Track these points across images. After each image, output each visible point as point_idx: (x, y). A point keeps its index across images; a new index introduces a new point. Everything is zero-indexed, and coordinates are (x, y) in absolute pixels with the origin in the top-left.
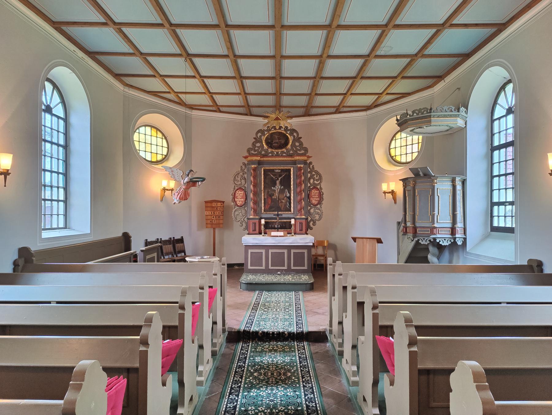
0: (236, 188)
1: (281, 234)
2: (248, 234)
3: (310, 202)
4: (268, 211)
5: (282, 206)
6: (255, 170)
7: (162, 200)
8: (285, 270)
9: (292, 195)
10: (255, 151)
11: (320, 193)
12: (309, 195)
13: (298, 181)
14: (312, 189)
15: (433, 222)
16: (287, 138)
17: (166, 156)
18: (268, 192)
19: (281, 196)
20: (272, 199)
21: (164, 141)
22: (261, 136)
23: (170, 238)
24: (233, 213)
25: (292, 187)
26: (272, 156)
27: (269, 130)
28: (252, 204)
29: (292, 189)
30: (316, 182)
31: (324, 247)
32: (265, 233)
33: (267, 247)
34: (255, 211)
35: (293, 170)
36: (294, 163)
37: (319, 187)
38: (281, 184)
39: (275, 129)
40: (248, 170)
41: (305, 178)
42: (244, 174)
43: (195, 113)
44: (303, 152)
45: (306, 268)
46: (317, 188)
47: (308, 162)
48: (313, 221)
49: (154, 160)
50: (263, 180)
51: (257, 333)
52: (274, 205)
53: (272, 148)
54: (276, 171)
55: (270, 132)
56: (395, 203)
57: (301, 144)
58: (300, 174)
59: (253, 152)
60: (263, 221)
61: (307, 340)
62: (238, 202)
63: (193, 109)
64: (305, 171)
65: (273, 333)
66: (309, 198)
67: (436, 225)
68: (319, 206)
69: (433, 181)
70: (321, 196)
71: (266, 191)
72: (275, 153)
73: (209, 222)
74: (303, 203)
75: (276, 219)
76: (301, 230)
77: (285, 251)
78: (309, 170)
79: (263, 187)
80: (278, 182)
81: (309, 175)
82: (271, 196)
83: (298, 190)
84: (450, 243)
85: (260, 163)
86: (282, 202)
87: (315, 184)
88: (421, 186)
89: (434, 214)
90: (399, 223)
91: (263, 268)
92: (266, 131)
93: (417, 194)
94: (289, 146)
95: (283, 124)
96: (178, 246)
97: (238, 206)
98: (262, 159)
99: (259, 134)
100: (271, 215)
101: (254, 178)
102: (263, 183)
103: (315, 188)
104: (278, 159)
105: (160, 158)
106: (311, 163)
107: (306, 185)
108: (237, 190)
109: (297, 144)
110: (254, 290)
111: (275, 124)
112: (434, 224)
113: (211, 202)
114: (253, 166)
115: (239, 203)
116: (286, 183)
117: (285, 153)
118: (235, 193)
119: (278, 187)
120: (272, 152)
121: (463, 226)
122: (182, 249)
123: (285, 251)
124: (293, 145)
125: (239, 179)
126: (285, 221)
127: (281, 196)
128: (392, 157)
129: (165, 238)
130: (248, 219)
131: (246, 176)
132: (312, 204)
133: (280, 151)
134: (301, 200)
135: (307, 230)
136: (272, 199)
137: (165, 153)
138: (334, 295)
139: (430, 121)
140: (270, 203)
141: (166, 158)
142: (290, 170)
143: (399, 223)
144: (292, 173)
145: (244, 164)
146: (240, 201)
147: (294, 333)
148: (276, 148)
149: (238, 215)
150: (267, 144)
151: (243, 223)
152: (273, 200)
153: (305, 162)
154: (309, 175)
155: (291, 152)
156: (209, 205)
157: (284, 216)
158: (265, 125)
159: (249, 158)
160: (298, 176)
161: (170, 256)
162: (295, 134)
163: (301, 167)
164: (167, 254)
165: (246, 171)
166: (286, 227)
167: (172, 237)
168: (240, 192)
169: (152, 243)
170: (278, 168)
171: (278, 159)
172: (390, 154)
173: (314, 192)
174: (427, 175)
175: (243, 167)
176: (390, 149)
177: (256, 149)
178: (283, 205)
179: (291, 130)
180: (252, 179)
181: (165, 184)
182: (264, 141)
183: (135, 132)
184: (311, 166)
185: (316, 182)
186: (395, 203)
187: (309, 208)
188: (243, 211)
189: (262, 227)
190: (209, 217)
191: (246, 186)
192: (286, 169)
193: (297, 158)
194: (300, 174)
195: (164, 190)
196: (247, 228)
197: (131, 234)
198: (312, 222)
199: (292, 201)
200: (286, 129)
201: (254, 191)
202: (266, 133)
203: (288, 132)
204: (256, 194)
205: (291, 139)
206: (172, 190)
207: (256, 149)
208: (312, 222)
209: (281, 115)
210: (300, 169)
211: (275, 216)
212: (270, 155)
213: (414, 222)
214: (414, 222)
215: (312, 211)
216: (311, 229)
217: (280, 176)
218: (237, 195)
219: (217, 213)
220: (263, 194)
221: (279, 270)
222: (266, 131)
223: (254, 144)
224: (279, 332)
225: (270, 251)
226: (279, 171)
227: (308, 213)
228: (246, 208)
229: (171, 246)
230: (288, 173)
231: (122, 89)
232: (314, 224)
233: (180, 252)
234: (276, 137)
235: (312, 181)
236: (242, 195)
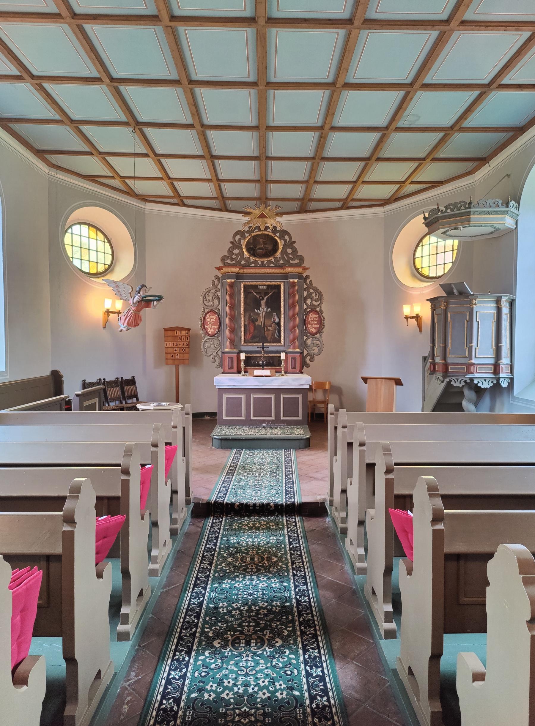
0: (207, 311)
1: (268, 372)
2: (223, 373)
3: (306, 330)
4: (248, 342)
6: (231, 285)
7: (105, 327)
8: (272, 421)
9: (282, 320)
10: (232, 260)
11: (320, 317)
12: (305, 320)
13: (291, 301)
14: (310, 312)
15: (470, 358)
16: (276, 242)
17: (110, 266)
18: (250, 316)
19: (268, 322)
20: (255, 326)
21: (107, 245)
22: (240, 240)
23: (117, 378)
24: (202, 344)
25: (282, 309)
26: (256, 267)
27: (250, 232)
28: (227, 332)
29: (282, 312)
30: (314, 303)
31: (325, 391)
32: (246, 372)
33: (248, 391)
34: (232, 342)
35: (284, 285)
36: (285, 276)
37: (318, 309)
38: (267, 305)
39: (260, 230)
40: (223, 286)
41: (301, 296)
42: (216, 291)
43: (150, 207)
44: (297, 261)
45: (300, 418)
46: (316, 311)
47: (304, 275)
48: (311, 356)
49: (94, 271)
51: (232, 504)
52: (258, 334)
53: (255, 256)
55: (253, 234)
56: (421, 331)
57: (295, 251)
58: (293, 292)
59: (229, 261)
60: (243, 356)
61: (300, 514)
62: (209, 330)
63: (146, 200)
64: (301, 287)
65: (255, 505)
66: (305, 324)
67: (474, 361)
68: (318, 336)
69: (470, 302)
70: (321, 321)
71: (247, 314)
72: (260, 263)
73: (169, 356)
74: (297, 331)
75: (260, 352)
76: (294, 368)
77: (273, 396)
78: (305, 286)
79: (242, 309)
80: (263, 303)
81: (305, 293)
82: (253, 321)
83: (291, 313)
84: (492, 385)
85: (238, 276)
86: (268, 330)
87: (314, 305)
88: (455, 308)
89: (471, 347)
90: (425, 359)
91: (243, 418)
92: (247, 232)
93: (449, 319)
94: (278, 254)
95: (270, 222)
96: (128, 389)
97: (209, 335)
98: (242, 271)
99: (238, 237)
100: (253, 347)
101: (231, 296)
102: (242, 304)
103: (313, 310)
104: (263, 270)
105: (101, 268)
106: (307, 277)
107: (301, 307)
108: (208, 313)
109: (289, 251)
110: (231, 448)
111: (259, 223)
112: (471, 359)
113: (173, 329)
114: (229, 281)
115: (210, 331)
116: (274, 304)
117: (273, 263)
118: (204, 318)
119: (263, 310)
120: (255, 262)
121: (509, 363)
122: (133, 393)
123: (273, 396)
124: (284, 252)
125: (210, 298)
126: (273, 355)
127: (268, 322)
128: (417, 270)
129: (110, 378)
130: (223, 353)
131: (219, 294)
132: (309, 333)
133: (265, 260)
134: (294, 327)
135: (302, 368)
136: (255, 326)
137: (108, 262)
138: (336, 455)
139: (469, 220)
140: (252, 330)
141: (109, 269)
142: (280, 286)
143: (425, 359)
144: (282, 290)
145: (217, 277)
146: (211, 328)
147: (282, 505)
148: (261, 256)
149: (209, 347)
150: (248, 250)
151: (216, 358)
152: (255, 327)
153: (299, 276)
154: (305, 293)
155: (281, 262)
156: (170, 333)
157: (271, 349)
158: (245, 224)
159: (224, 270)
160: (290, 295)
161: (117, 402)
162: (287, 237)
163: (294, 282)
164: (113, 400)
165: (219, 287)
166: (273, 363)
167: (119, 377)
168: (211, 316)
169: (91, 384)
170: (263, 284)
171: (262, 271)
172: (415, 266)
173: (312, 317)
174: (463, 293)
175: (216, 282)
176: (414, 259)
177: (234, 257)
178: (270, 333)
179: (280, 231)
180: (228, 298)
181: (108, 304)
182: (244, 247)
183: (66, 232)
184: (308, 281)
185: (314, 303)
186: (421, 331)
187: (305, 338)
188: (216, 343)
189: (242, 363)
190: (170, 350)
191: (220, 307)
192: (275, 285)
193: (289, 270)
194: (293, 292)
195: (108, 312)
196: (221, 365)
197: (62, 373)
198: (309, 358)
199: (282, 329)
200: (275, 229)
201: (231, 315)
202: (247, 235)
203: (278, 234)
204: (233, 318)
205: (281, 243)
206: (119, 313)
207: (234, 257)
208: (309, 358)
209: (267, 211)
210: (293, 285)
211: (259, 349)
212: (253, 265)
213: (445, 357)
214: (445, 357)
215: (309, 342)
216: (308, 366)
217: (266, 294)
218: (207, 320)
219: (181, 344)
220: (243, 319)
221: (264, 421)
222: (247, 232)
223: (230, 251)
224: (263, 504)
225: (253, 396)
226: (265, 287)
227: (304, 345)
228: (220, 338)
229: (118, 389)
230: (276, 291)
231: (47, 171)
232: (312, 360)
233: (131, 397)
234: (261, 240)
235: (309, 301)
236: (214, 320)
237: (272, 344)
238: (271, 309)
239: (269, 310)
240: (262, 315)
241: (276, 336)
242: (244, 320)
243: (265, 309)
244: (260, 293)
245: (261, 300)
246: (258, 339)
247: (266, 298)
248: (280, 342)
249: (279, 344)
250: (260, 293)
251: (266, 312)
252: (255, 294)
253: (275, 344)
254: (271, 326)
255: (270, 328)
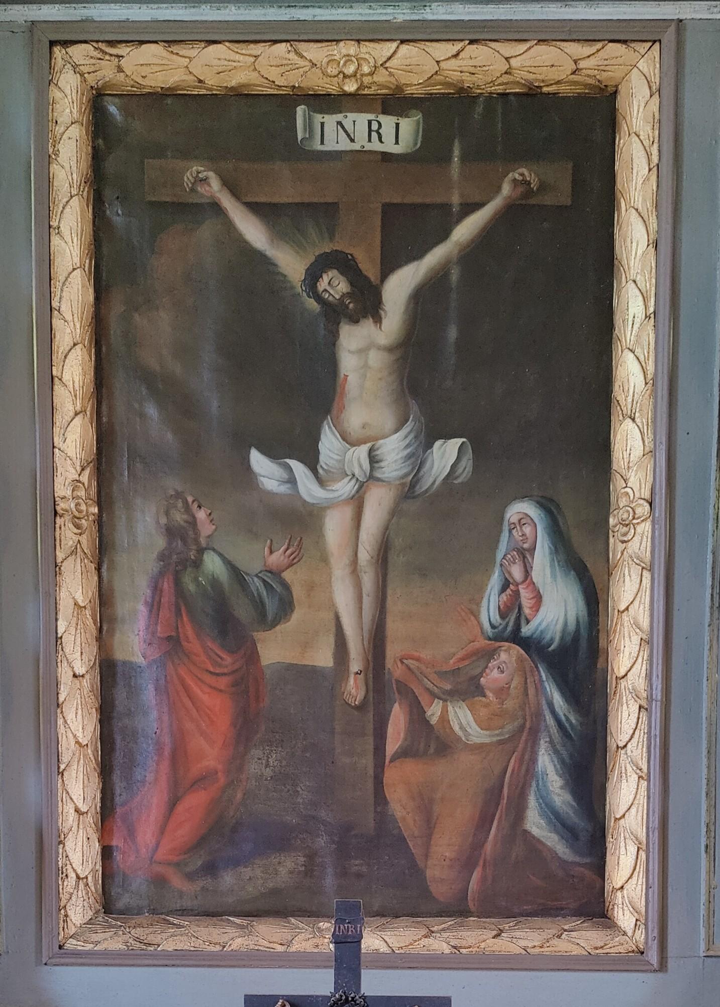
4: (162, 908)
5: (433, 808)
9: (632, 595)
18: (181, 552)
19: (423, 635)
20: (247, 683)
25: (632, 443)
35: (673, 93)
38: (424, 383)
50: (74, 296)
54: (340, 133)
71: (144, 529)
79: (73, 440)
80: (364, 354)
82: (222, 617)
86: (430, 741)
102: (74, 371)
116: (521, 373)
119: (368, 446)
136: (247, 683)
140: (209, 753)
178: (458, 785)
199: (627, 722)
217: (409, 229)
220: (75, 587)
226: (398, 135)
230: (551, 178)
237: (476, 937)
238: (479, 446)
239: (446, 454)
240: (348, 538)
241: (535, 823)
242: (105, 599)
243: (394, 449)
244: (325, 214)
245: (335, 314)
246: (285, 868)
247: (399, 287)
248: (595, 908)
249: (584, 939)
250: (325, 214)
251: (409, 490)
252: (253, 232)
253: (526, 938)
254: (468, 688)
255: (463, 719)
